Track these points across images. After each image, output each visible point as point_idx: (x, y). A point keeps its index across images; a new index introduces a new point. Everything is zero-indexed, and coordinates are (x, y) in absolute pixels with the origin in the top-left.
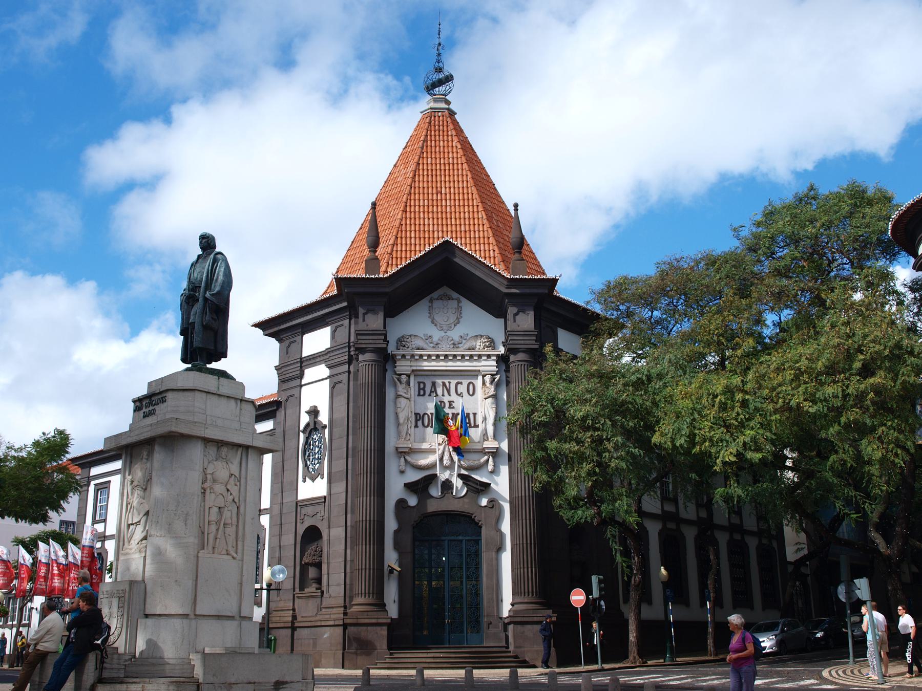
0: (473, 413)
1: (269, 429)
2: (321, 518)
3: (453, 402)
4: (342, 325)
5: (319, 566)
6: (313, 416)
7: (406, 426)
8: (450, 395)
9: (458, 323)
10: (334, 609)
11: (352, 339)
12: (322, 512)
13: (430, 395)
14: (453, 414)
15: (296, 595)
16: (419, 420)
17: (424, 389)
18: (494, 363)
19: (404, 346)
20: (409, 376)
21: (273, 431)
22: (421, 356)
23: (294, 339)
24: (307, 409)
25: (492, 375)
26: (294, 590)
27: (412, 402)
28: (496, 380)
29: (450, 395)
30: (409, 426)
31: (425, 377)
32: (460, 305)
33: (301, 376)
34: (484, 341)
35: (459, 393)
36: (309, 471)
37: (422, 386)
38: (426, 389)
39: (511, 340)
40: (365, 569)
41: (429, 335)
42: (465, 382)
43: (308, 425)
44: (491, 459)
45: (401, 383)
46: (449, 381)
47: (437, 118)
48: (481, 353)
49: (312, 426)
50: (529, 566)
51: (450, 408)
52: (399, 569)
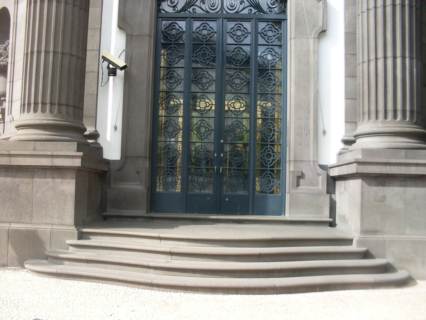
40: (39, 52)
50: (399, 53)
52: (122, 63)
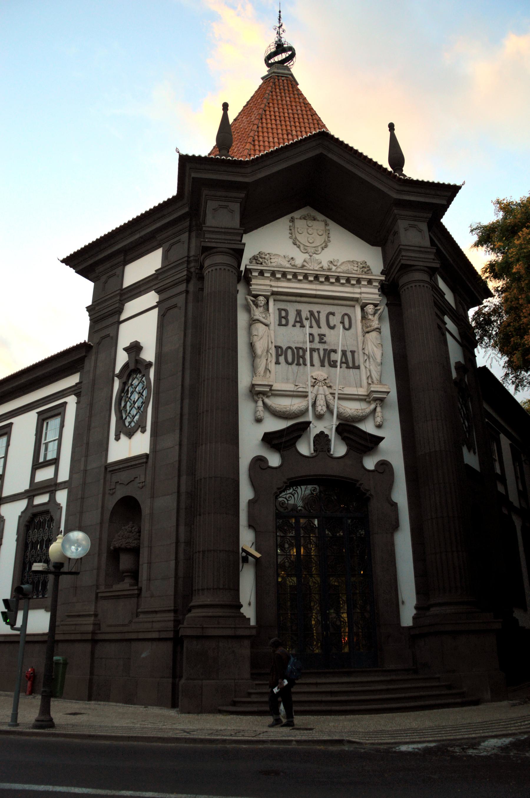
0: (351, 351)
1: (74, 384)
2: (141, 485)
3: (324, 335)
4: (179, 241)
5: (135, 551)
6: (134, 354)
7: (265, 361)
8: (319, 327)
9: (326, 246)
10: (158, 615)
11: (192, 253)
12: (143, 477)
13: (294, 326)
14: (325, 350)
15: (100, 595)
16: (281, 355)
17: (286, 318)
18: (376, 291)
19: (261, 264)
20: (267, 298)
21: (79, 385)
22: (284, 274)
23: (113, 272)
24: (127, 344)
25: (376, 305)
26: (97, 587)
27: (272, 332)
28: (379, 312)
29: (319, 327)
30: (269, 360)
31: (288, 304)
32: (328, 228)
33: (120, 311)
34: (362, 266)
35: (332, 324)
36: (125, 425)
37: (283, 314)
38: (289, 318)
39: (402, 256)
41: (290, 257)
42: (339, 311)
43: (126, 366)
44: (379, 409)
45: (257, 306)
46: (318, 310)
47: (281, 81)
48: (360, 276)
49: (132, 366)
51: (320, 342)
